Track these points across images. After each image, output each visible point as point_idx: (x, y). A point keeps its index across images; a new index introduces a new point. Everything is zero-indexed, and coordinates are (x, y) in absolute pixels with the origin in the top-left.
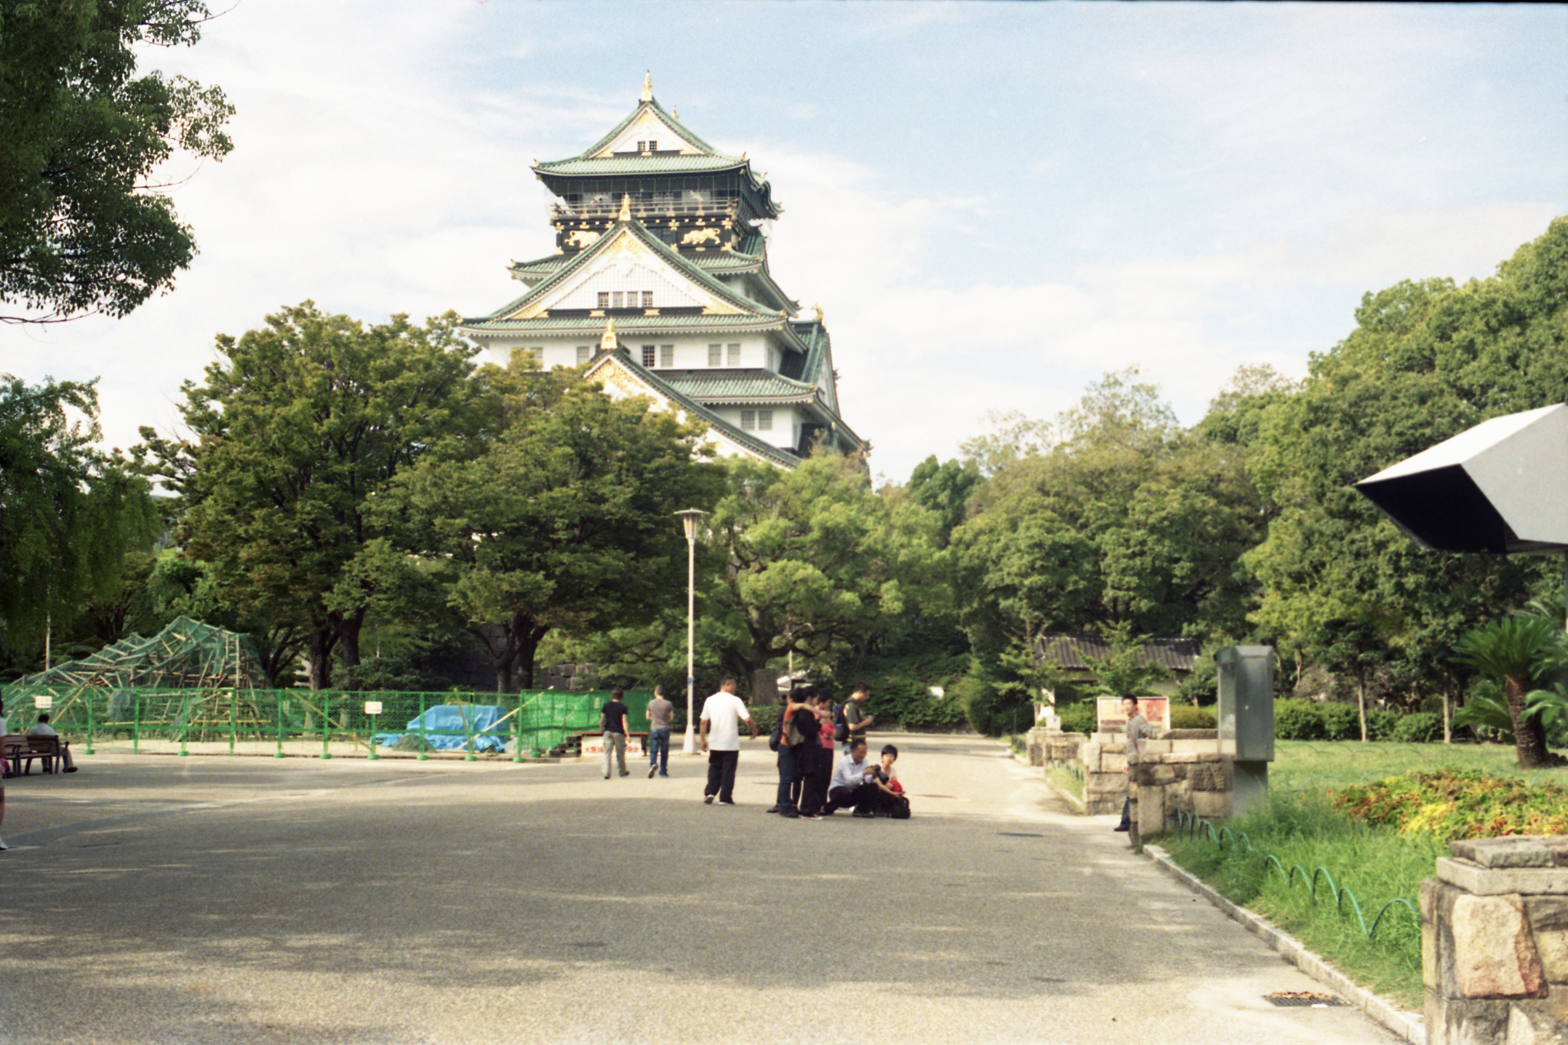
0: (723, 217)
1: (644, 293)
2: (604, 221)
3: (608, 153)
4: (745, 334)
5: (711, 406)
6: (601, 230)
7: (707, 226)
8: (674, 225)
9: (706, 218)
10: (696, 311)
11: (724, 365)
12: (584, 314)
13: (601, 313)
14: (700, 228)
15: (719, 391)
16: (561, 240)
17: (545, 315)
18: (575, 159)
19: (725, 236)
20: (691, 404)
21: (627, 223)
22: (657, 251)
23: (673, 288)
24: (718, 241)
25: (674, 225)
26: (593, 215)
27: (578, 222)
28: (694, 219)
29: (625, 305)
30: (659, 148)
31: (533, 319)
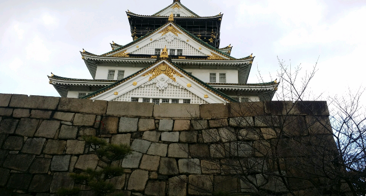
0: (210, 38)
1: (178, 50)
10: (205, 57)
11: (218, 81)
12: (149, 56)
21: (172, 21)
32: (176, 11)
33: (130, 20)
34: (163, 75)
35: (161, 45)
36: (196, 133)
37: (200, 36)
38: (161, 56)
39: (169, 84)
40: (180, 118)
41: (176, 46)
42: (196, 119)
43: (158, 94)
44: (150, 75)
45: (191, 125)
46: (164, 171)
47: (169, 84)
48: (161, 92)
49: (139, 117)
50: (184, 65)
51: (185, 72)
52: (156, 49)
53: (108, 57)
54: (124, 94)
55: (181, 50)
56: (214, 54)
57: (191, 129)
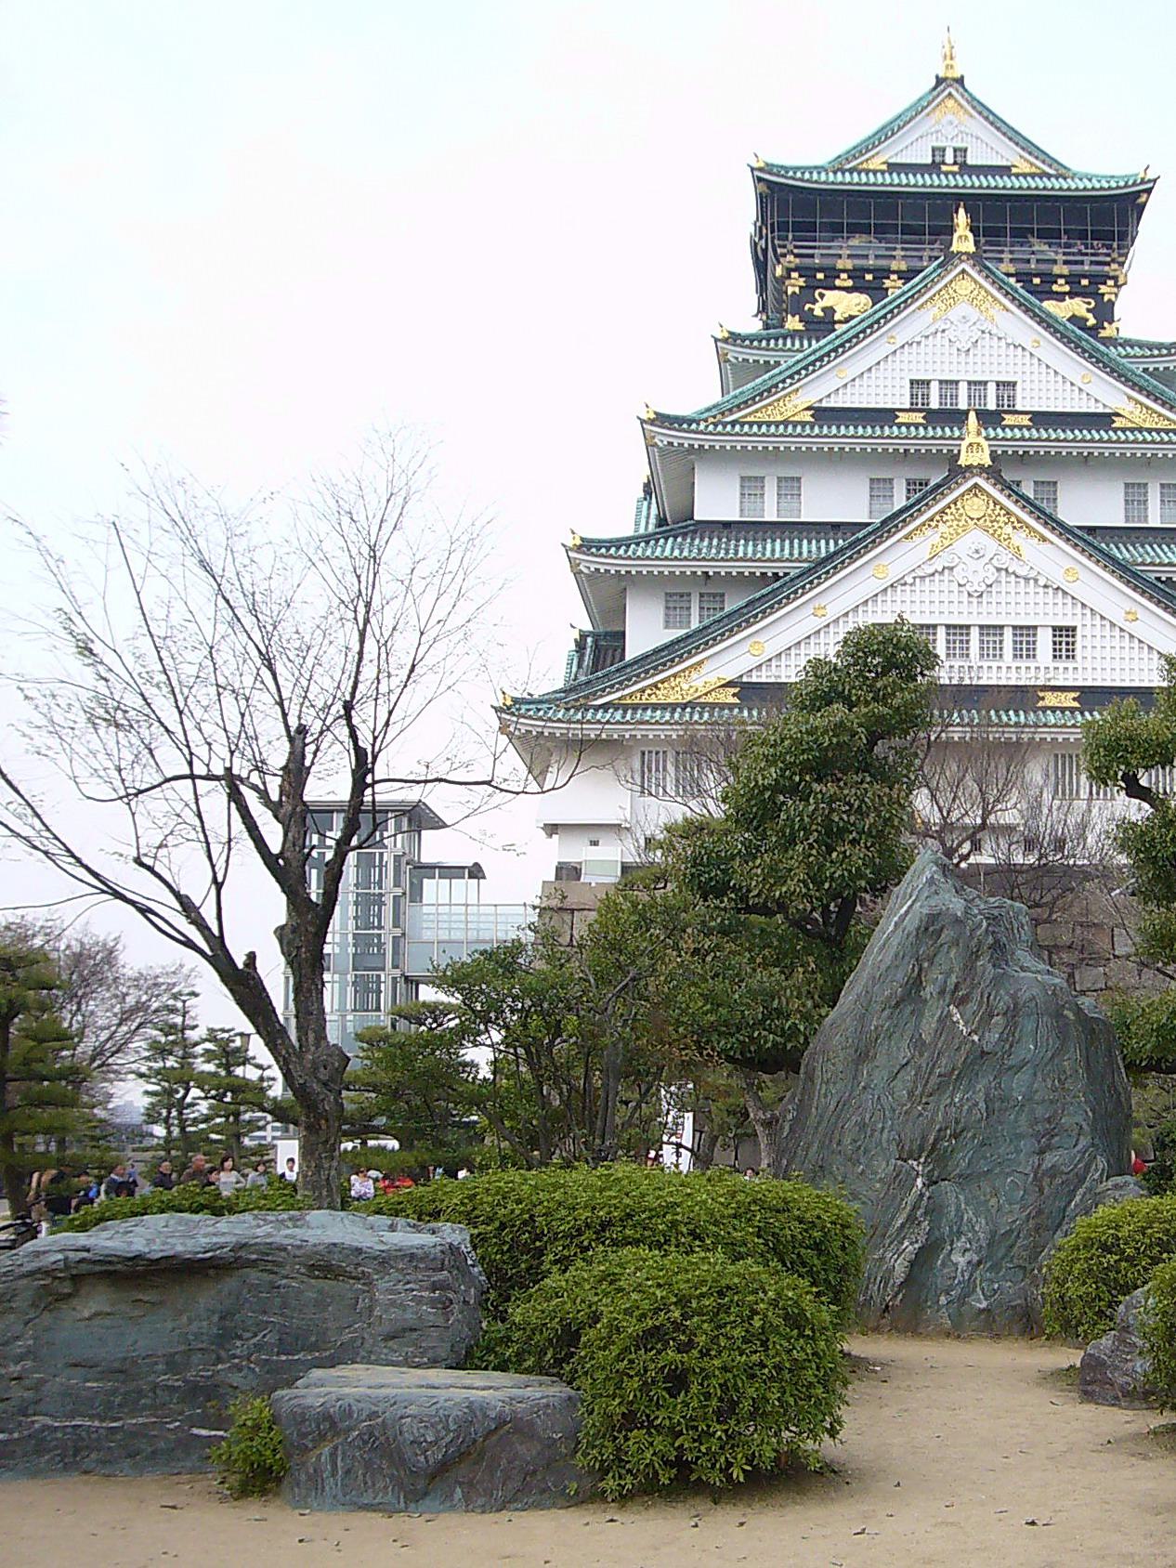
0: (1104, 278)
2: (886, 273)
3: (876, 164)
6: (876, 292)
7: (1072, 294)
10: (1103, 420)
12: (884, 416)
13: (918, 418)
14: (1060, 297)
17: (807, 417)
18: (819, 169)
20: (1135, 575)
23: (1054, 379)
24: (1092, 321)
26: (859, 262)
27: (833, 273)
28: (1050, 279)
30: (969, 162)
31: (786, 423)
33: (762, 200)
34: (976, 538)
35: (937, 363)
37: (1065, 270)
38: (962, 461)
39: (999, 570)
43: (964, 608)
44: (931, 538)
47: (999, 570)
48: (975, 600)
50: (1033, 458)
52: (912, 382)
53: (733, 423)
54: (846, 614)
55: (1015, 384)
56: (1137, 402)
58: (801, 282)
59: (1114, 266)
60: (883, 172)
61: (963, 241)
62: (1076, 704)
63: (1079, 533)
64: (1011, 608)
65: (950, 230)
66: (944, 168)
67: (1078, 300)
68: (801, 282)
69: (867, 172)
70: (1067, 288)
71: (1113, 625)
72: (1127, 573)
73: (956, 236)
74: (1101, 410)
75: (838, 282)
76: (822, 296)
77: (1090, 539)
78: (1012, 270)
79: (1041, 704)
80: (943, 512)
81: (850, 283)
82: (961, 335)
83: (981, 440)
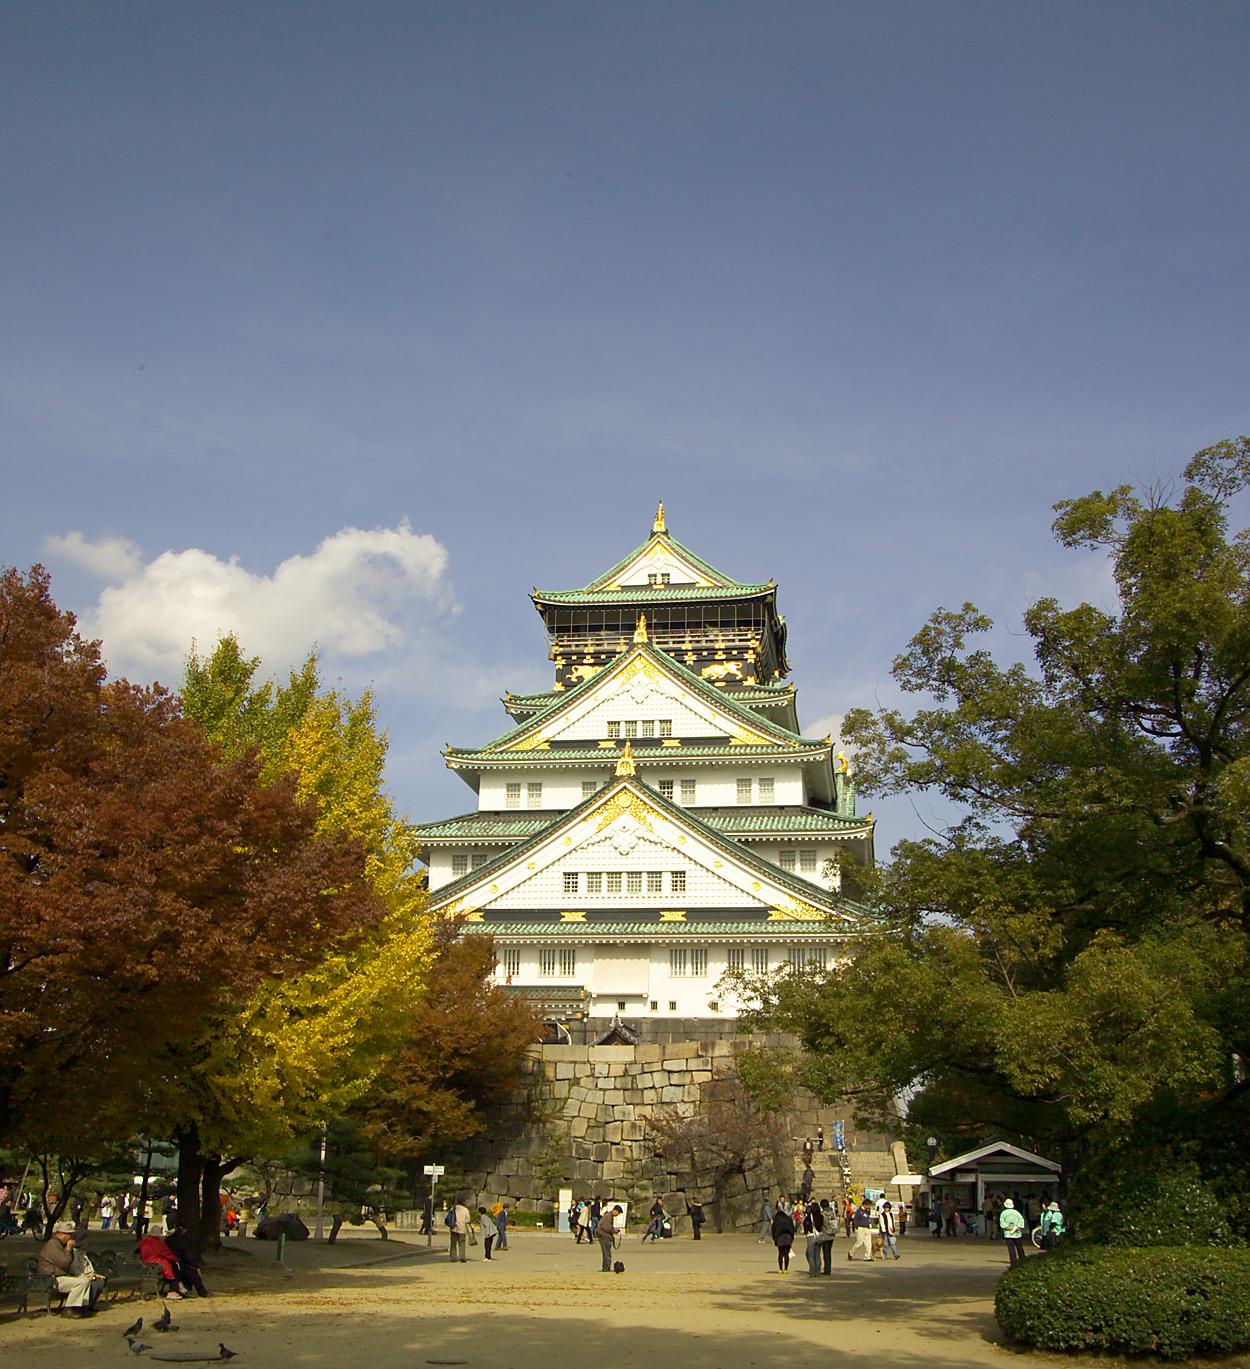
3: (612, 588)
4: (778, 766)
5: (747, 842)
7: (727, 660)
8: (690, 658)
9: (727, 651)
10: (724, 741)
12: (592, 744)
15: (754, 826)
16: (561, 676)
17: (546, 746)
19: (748, 670)
20: (723, 839)
22: (677, 675)
23: (693, 718)
25: (690, 658)
27: (582, 655)
28: (713, 651)
29: (639, 735)
31: (533, 750)
32: (659, 564)
33: (542, 613)
34: (626, 819)
35: (623, 711)
36: (630, 1079)
37: (722, 645)
38: (618, 773)
40: (616, 1063)
41: (656, 709)
42: (631, 1064)
44: (597, 819)
45: (626, 1070)
46: (602, 1120)
49: (575, 1062)
51: (668, 806)
53: (501, 752)
57: (626, 1073)
58: (563, 662)
59: (753, 641)
60: (617, 592)
61: (640, 635)
62: (684, 919)
63: (688, 812)
64: (646, 859)
65: (633, 628)
66: (655, 587)
67: (733, 663)
68: (563, 662)
69: (608, 592)
70: (724, 657)
71: (708, 870)
72: (716, 837)
73: (636, 633)
74: (722, 734)
75: (585, 661)
76: (576, 669)
77: (693, 818)
78: (689, 646)
79: (662, 919)
80: (605, 803)
81: (592, 661)
82: (641, 694)
83: (631, 760)
